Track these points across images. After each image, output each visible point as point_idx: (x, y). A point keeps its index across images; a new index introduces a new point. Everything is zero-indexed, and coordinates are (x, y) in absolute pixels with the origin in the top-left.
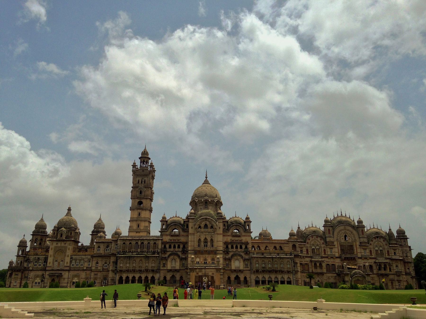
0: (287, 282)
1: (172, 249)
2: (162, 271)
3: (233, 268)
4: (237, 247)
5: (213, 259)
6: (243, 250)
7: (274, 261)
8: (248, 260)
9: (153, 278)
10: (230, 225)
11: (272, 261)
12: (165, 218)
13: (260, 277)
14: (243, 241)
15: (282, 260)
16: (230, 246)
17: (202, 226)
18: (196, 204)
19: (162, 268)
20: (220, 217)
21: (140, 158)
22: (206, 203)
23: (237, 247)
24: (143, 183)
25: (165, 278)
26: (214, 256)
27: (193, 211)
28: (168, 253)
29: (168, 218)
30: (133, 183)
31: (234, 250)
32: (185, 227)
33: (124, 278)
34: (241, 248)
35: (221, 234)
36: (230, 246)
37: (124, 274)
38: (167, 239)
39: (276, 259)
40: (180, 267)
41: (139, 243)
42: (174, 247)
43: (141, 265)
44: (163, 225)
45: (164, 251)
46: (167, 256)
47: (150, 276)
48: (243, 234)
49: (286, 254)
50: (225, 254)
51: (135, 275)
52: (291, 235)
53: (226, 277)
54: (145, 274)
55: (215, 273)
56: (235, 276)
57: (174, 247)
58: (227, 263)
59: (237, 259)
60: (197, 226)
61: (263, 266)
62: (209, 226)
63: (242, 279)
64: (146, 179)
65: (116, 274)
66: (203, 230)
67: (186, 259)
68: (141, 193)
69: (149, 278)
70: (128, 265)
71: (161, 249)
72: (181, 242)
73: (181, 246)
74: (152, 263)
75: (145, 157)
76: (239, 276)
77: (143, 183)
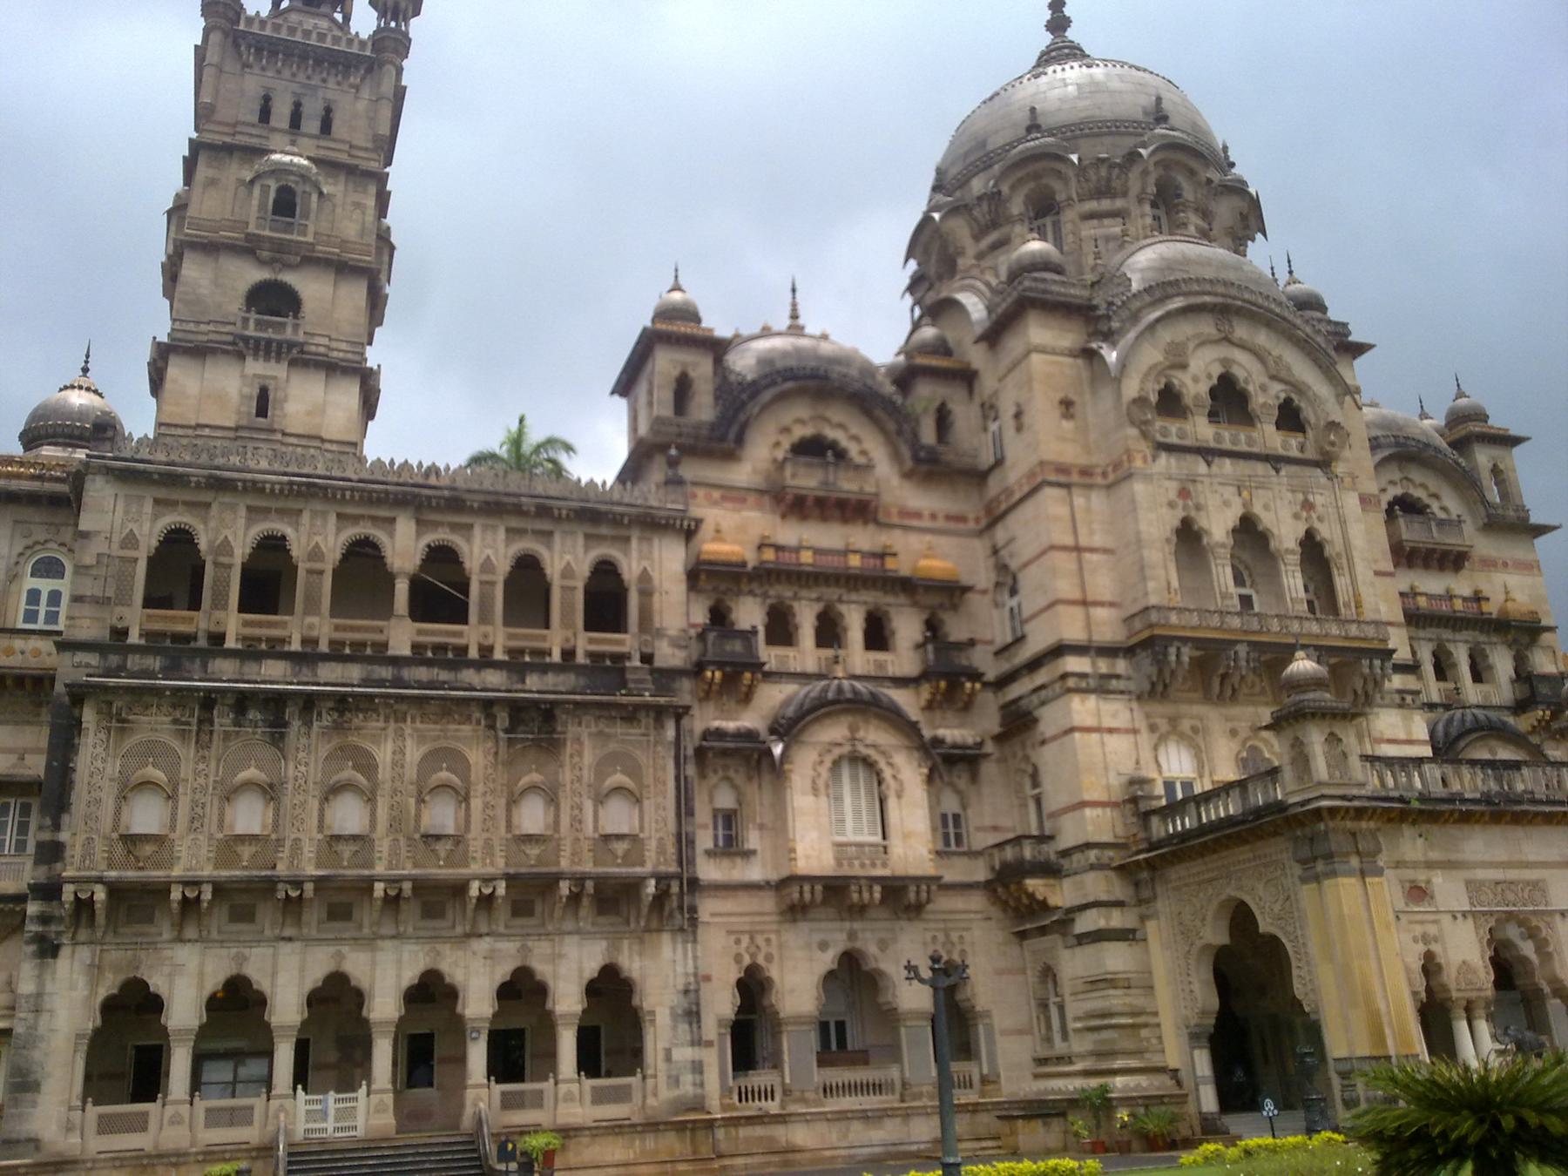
1: (806, 654)
9: (611, 991)
12: (695, 317)
19: (709, 871)
25: (752, 987)
28: (773, 698)
33: (184, 1010)
37: (188, 956)
41: (404, 547)
43: (442, 816)
46: (751, 719)
47: (568, 968)
51: (357, 965)
54: (509, 947)
57: (829, 632)
65: (48, 950)
68: (285, 205)
69: (568, 1000)
70: (249, 817)
73: (907, 627)
74: (600, 800)
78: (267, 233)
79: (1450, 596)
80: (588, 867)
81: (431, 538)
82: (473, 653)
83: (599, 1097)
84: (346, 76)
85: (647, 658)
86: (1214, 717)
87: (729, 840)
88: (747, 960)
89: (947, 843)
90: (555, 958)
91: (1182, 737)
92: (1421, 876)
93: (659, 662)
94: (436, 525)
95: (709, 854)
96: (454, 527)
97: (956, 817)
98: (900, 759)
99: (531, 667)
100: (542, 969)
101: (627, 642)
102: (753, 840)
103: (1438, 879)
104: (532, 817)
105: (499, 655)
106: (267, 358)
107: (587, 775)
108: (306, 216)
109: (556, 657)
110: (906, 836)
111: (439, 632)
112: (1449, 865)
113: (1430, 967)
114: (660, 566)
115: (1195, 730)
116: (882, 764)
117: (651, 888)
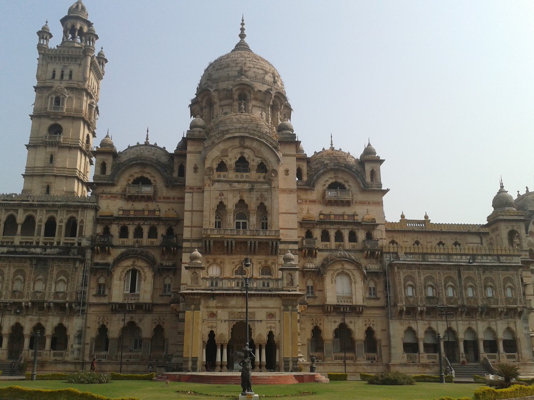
0: (505, 342)
1: (130, 240)
2: (92, 310)
3: (331, 299)
4: (339, 237)
5: (266, 270)
6: (358, 245)
7: (463, 277)
8: (375, 274)
9: (61, 330)
10: (317, 170)
11: (456, 277)
13: (420, 328)
14: (359, 219)
15: (488, 274)
16: (317, 233)
17: (231, 161)
18: (211, 104)
20: (291, 141)
21: (63, 21)
22: (243, 98)
23: (339, 237)
24: (66, 77)
25: (103, 330)
26: (271, 259)
27: (200, 121)
28: (116, 253)
29: (120, 147)
30: (38, 77)
31: (333, 244)
32: (176, 174)
34: (353, 237)
35: (291, 191)
36: (317, 233)
38: (111, 206)
39: (471, 273)
40: (152, 297)
41: (21, 217)
42: (139, 233)
43: (18, 286)
44: (103, 167)
45: (102, 244)
46: (110, 260)
47: (51, 323)
48: (360, 197)
49: (498, 256)
50: (304, 256)
52: (501, 201)
53: (309, 328)
55: (277, 312)
56: (335, 326)
58: (310, 283)
59: (343, 273)
60: (211, 162)
61: (430, 293)
62: (254, 162)
63: (359, 334)
64: (75, 68)
66: (231, 175)
67: (175, 270)
68: (58, 101)
69: (49, 331)
71: (93, 239)
72: (159, 219)
73: (162, 231)
75: (76, 23)
76: (351, 326)
77: (66, 77)
78: (52, 111)
79: (343, 215)
80: (51, 299)
81: (27, 214)
82: (34, 244)
83: (55, 355)
84: (76, 61)
85: (79, 244)
86: (227, 258)
87: (100, 291)
88: (101, 323)
89: (165, 291)
90: (47, 321)
91: (217, 264)
92: (214, 311)
93: (82, 245)
94: (28, 210)
95: (94, 296)
96: (33, 211)
97: (169, 285)
98: (146, 270)
99: (48, 247)
100: (43, 323)
101: (76, 240)
102: (107, 292)
103: (220, 311)
104: (39, 286)
105: (41, 244)
106: (52, 147)
107: (54, 277)
108: (63, 105)
109: (55, 244)
110: (145, 292)
111: (28, 238)
112: (223, 307)
113: (212, 335)
114: (87, 220)
115: (221, 262)
116: (141, 272)
117: (67, 305)
